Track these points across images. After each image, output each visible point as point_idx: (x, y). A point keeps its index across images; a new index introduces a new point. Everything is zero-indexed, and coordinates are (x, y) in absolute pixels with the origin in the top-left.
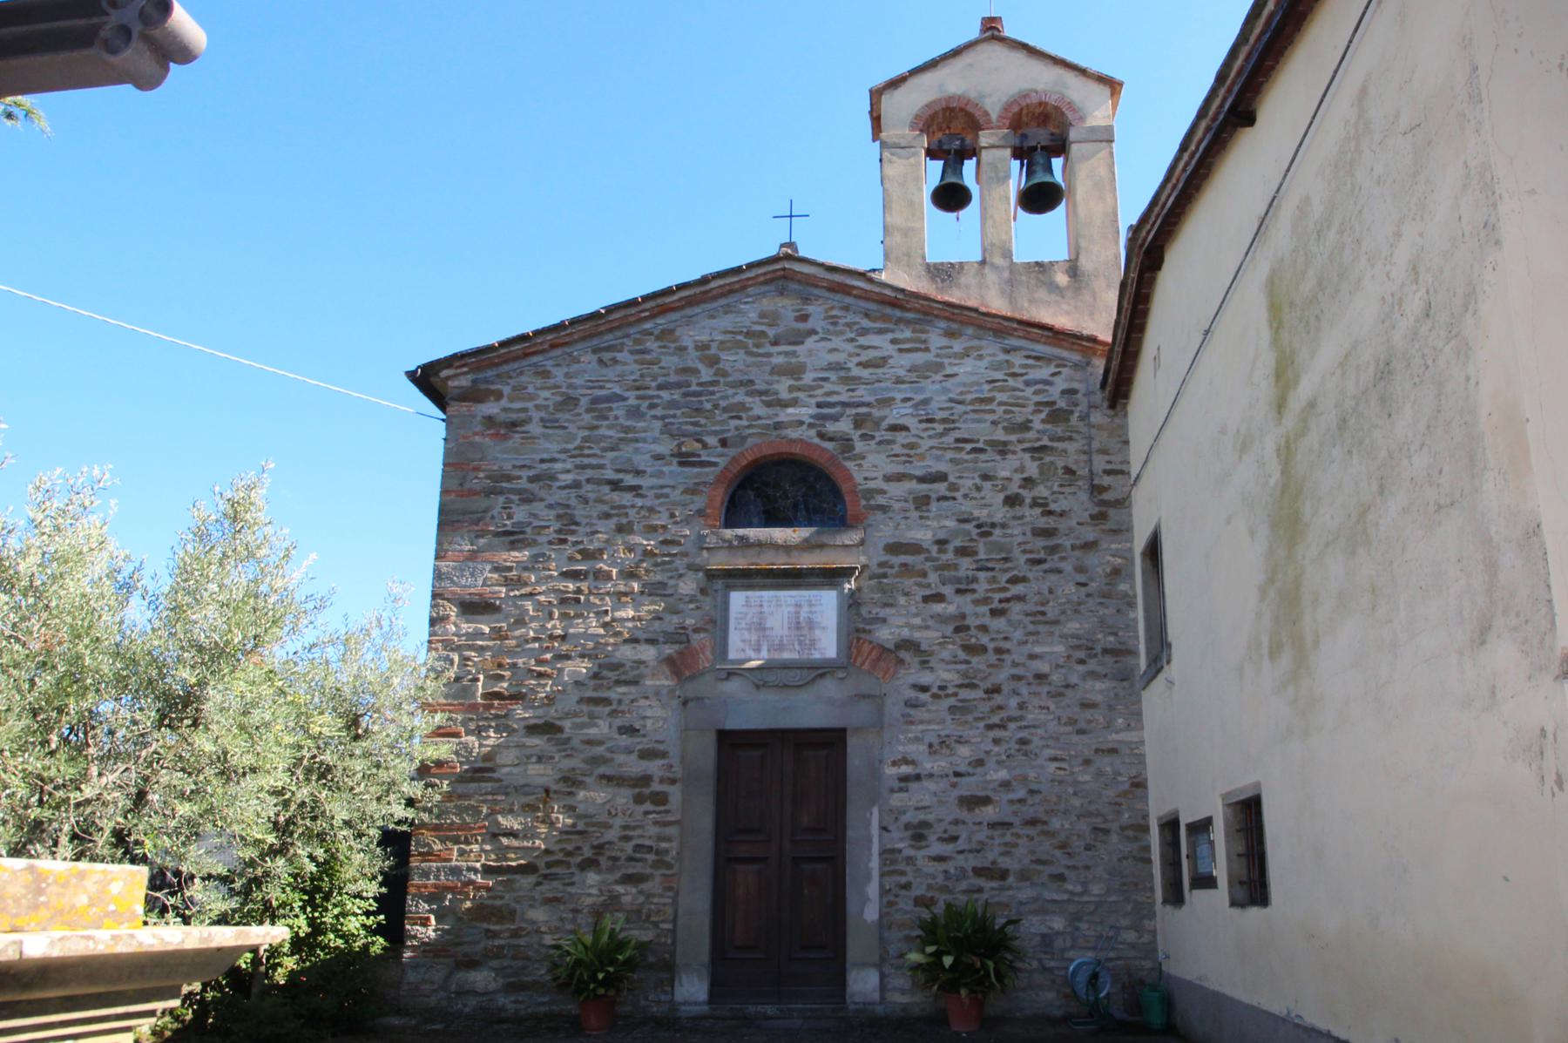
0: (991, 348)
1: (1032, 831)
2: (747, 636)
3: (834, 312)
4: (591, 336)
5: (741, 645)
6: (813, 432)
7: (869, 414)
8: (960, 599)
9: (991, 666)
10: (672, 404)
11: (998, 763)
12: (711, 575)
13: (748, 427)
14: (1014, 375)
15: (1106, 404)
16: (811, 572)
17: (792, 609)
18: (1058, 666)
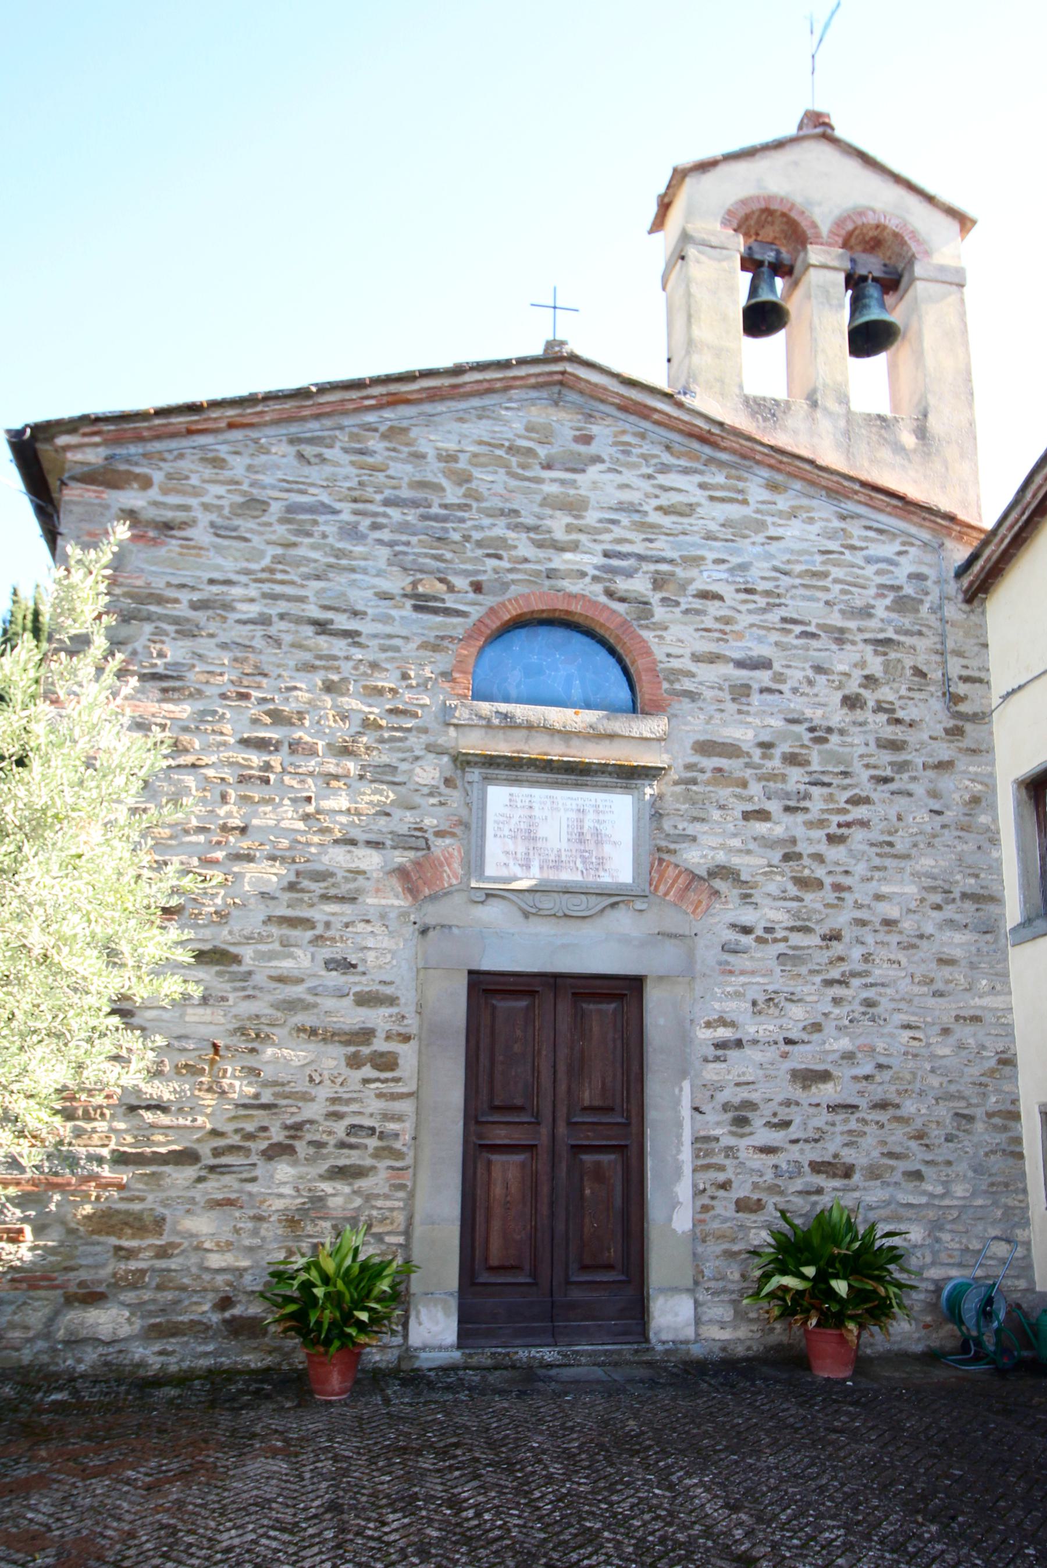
0: (824, 510)
1: (883, 1116)
2: (511, 847)
3: (626, 438)
4: (290, 420)
5: (503, 859)
6: (598, 588)
7: (672, 574)
8: (788, 819)
9: (827, 906)
10: (404, 527)
11: (839, 1028)
12: (463, 762)
13: (510, 571)
14: (853, 548)
15: (961, 597)
16: (603, 769)
17: (573, 815)
18: (909, 911)
